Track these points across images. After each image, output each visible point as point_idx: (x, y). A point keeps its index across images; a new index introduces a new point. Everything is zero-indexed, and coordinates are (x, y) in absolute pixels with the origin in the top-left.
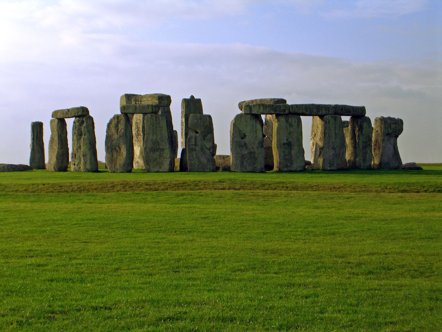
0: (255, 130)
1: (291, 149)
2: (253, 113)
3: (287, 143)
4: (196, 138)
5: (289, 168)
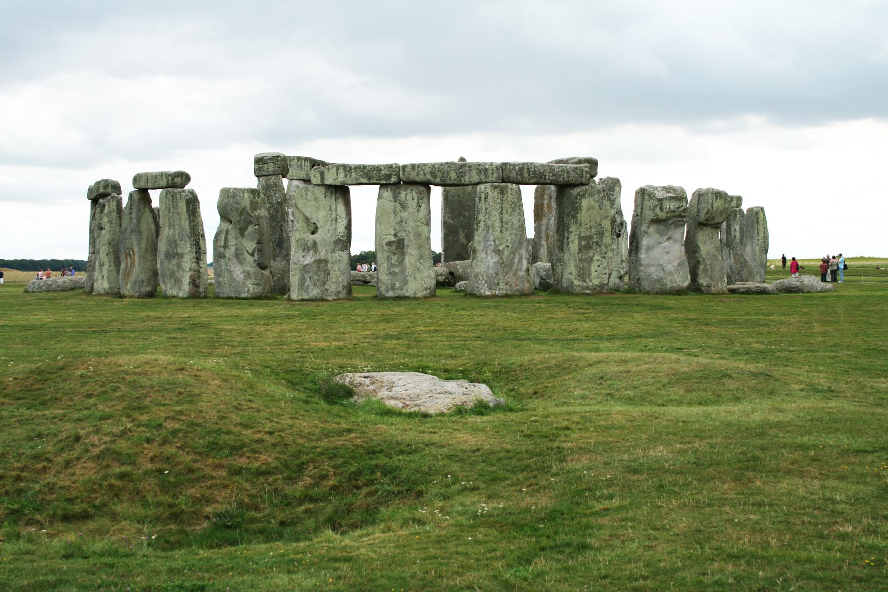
0: (334, 216)
1: (403, 253)
2: (327, 182)
3: (394, 242)
4: (227, 233)
5: (399, 293)
